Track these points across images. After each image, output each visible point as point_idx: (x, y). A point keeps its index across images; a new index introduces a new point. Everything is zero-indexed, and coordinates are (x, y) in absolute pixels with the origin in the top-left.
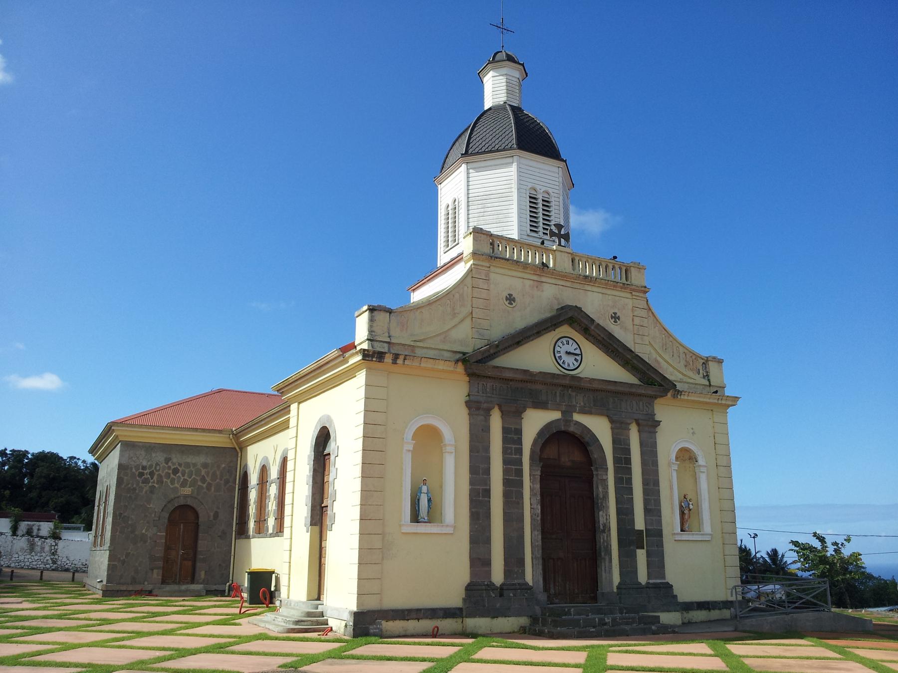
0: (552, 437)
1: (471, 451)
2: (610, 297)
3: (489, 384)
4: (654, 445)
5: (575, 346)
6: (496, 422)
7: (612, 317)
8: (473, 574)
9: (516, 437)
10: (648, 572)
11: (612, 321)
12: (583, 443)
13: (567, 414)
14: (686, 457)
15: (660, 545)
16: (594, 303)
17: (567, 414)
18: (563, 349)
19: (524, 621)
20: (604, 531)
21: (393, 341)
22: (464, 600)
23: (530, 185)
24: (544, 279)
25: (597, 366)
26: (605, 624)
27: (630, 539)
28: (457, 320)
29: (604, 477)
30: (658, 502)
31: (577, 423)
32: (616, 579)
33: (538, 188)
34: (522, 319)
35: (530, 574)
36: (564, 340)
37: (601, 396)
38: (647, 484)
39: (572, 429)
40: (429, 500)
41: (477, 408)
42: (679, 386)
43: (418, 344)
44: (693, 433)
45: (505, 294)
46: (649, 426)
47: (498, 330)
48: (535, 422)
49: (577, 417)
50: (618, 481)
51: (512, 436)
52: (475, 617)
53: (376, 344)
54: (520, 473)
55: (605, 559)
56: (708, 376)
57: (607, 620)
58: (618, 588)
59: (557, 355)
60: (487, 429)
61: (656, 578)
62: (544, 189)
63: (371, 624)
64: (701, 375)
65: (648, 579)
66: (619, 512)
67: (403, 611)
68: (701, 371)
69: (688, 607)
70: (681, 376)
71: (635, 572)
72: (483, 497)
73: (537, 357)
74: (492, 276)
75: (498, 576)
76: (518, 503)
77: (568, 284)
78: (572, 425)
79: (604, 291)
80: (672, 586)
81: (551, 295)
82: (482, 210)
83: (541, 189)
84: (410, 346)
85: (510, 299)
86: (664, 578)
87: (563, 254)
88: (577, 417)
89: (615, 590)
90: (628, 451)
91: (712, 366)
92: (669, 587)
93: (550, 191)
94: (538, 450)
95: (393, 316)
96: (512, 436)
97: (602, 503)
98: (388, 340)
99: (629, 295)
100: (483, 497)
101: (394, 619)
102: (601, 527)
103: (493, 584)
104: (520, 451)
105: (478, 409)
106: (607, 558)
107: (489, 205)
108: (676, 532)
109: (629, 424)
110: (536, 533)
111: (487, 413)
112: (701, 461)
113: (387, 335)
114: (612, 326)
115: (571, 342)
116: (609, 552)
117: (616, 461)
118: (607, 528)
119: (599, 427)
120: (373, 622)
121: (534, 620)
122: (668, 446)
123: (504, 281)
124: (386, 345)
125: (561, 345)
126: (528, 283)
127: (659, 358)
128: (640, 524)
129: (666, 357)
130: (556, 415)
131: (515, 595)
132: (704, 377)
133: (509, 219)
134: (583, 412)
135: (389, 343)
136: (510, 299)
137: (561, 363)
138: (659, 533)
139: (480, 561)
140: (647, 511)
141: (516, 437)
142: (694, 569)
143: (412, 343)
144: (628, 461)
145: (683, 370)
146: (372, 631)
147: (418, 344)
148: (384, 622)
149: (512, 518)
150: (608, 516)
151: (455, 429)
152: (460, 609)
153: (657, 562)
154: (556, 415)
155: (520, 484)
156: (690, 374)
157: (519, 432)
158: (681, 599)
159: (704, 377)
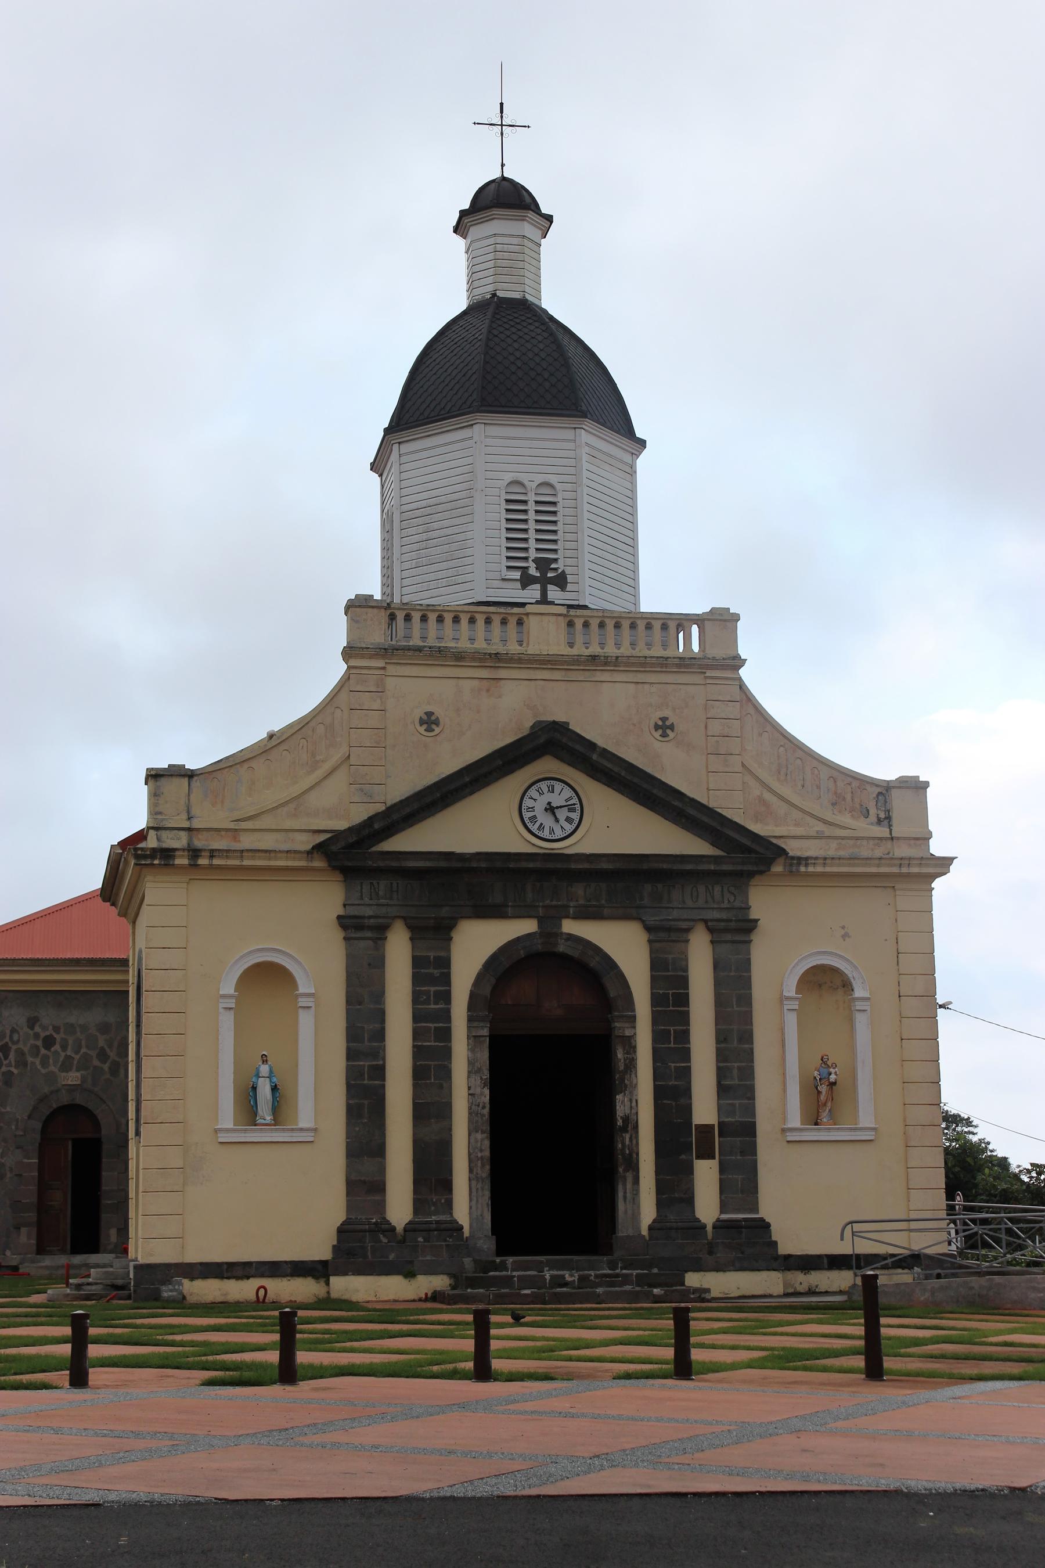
0: (503, 969)
1: (349, 1002)
2: (654, 689)
3: (383, 885)
4: (746, 965)
5: (568, 793)
6: (399, 951)
7: (657, 727)
8: (350, 1207)
9: (436, 972)
10: (721, 1201)
11: (657, 735)
12: (595, 973)
13: (549, 921)
14: (824, 981)
15: (750, 1149)
16: (604, 713)
17: (549, 921)
18: (537, 802)
19: (440, 1282)
20: (624, 1129)
21: (196, 824)
22: (335, 1248)
23: (509, 477)
24: (503, 673)
25: (616, 828)
26: (566, 1284)
27: (678, 1141)
28: (319, 773)
29: (628, 1033)
30: (748, 1072)
31: (571, 937)
32: (648, 1212)
33: (523, 478)
34: (450, 758)
35: (466, 1205)
36: (543, 785)
37: (624, 883)
38: (725, 1040)
39: (561, 948)
40: (274, 1089)
41: (360, 930)
42: (793, 848)
43: (244, 825)
44: (845, 936)
45: (419, 713)
46: (736, 932)
47: (403, 783)
48: (476, 944)
49: (569, 927)
50: (659, 1037)
51: (431, 975)
52: (345, 1274)
53: (164, 834)
54: (445, 1034)
55: (625, 1179)
56: (889, 818)
57: (568, 1278)
58: (651, 1228)
59: (527, 815)
60: (378, 963)
61: (744, 1211)
62: (540, 479)
63: (164, 1283)
64: (873, 818)
65: (721, 1212)
66: (660, 1093)
67: (219, 1265)
68: (873, 812)
69: (808, 1263)
70: (820, 827)
71: (689, 1200)
72: (370, 1078)
73: (484, 827)
74: (390, 683)
75: (399, 1207)
76: (441, 1087)
77: (557, 675)
78: (561, 941)
79: (640, 677)
80: (768, 1225)
81: (510, 708)
82: (424, 536)
83: (532, 480)
84: (227, 830)
85: (429, 721)
86: (756, 1210)
87: (546, 618)
88: (569, 927)
89: (645, 1232)
90: (683, 981)
91: (898, 801)
92: (764, 1226)
93: (553, 479)
94: (487, 991)
95: (196, 783)
96: (431, 975)
97: (622, 1080)
98: (186, 825)
99: (698, 679)
100: (370, 1078)
101: (204, 1276)
102: (620, 1123)
103: (388, 1223)
104: (446, 997)
105: (359, 928)
106: (629, 1176)
107: (435, 525)
108: (790, 1125)
109: (688, 930)
110: (479, 1136)
111: (381, 930)
112: (859, 993)
113: (185, 816)
114: (657, 745)
115: (558, 786)
116: (633, 1165)
117: (656, 1000)
118: (631, 1124)
119: (623, 945)
120: (166, 1281)
121: (458, 1280)
122: (776, 967)
123: (414, 689)
124: (183, 835)
125: (545, 789)
126: (467, 685)
127: (767, 796)
128: (705, 1109)
129: (786, 791)
130: (527, 927)
131: (426, 1240)
132: (879, 821)
133: (469, 552)
134: (587, 914)
135: (189, 829)
136: (429, 721)
137: (534, 828)
138: (749, 1130)
139: (365, 1184)
140: (723, 1090)
141: (436, 972)
142: (822, 1194)
143: (232, 826)
144: (683, 1000)
145: (828, 816)
146: (165, 1294)
147: (244, 825)
148: (186, 1282)
149: (431, 1110)
150: (634, 1103)
151: (319, 967)
152: (324, 1263)
153: (741, 1181)
154: (527, 927)
155: (446, 1053)
156: (846, 819)
157: (445, 963)
158: (783, 1249)
159: (879, 821)
